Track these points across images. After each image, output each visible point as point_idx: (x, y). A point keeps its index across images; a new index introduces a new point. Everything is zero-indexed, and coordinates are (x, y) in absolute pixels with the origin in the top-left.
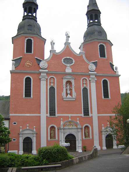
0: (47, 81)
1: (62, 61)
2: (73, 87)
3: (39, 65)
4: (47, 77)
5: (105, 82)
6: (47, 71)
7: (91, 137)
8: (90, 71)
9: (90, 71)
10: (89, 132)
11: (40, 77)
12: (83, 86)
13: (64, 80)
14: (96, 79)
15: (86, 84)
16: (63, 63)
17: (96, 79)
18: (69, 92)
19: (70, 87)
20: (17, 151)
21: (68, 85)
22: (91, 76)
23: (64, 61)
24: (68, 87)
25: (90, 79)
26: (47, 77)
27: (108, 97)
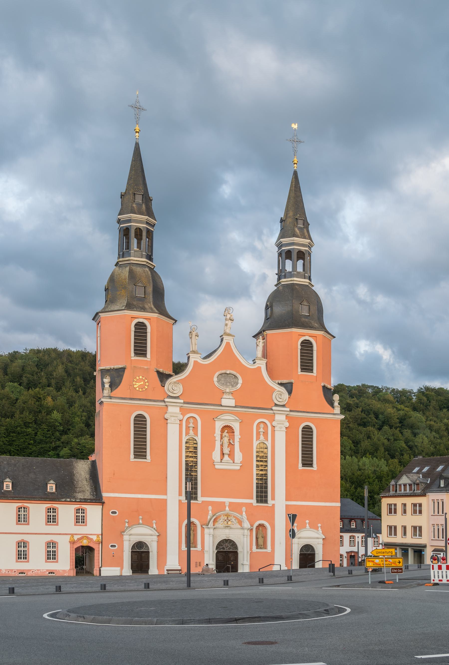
0: (181, 425)
1: (215, 379)
3: (164, 386)
4: (181, 417)
5: (307, 432)
6: (182, 401)
7: (269, 549)
8: (276, 405)
9: (276, 405)
10: (265, 538)
11: (166, 416)
12: (258, 438)
13: (216, 422)
14: (287, 424)
15: (265, 434)
16: (216, 383)
17: (287, 424)
18: (226, 450)
19: (229, 440)
21: (225, 434)
22: (277, 417)
23: (219, 381)
24: (226, 440)
25: (274, 423)
26: (181, 417)
27: (311, 465)
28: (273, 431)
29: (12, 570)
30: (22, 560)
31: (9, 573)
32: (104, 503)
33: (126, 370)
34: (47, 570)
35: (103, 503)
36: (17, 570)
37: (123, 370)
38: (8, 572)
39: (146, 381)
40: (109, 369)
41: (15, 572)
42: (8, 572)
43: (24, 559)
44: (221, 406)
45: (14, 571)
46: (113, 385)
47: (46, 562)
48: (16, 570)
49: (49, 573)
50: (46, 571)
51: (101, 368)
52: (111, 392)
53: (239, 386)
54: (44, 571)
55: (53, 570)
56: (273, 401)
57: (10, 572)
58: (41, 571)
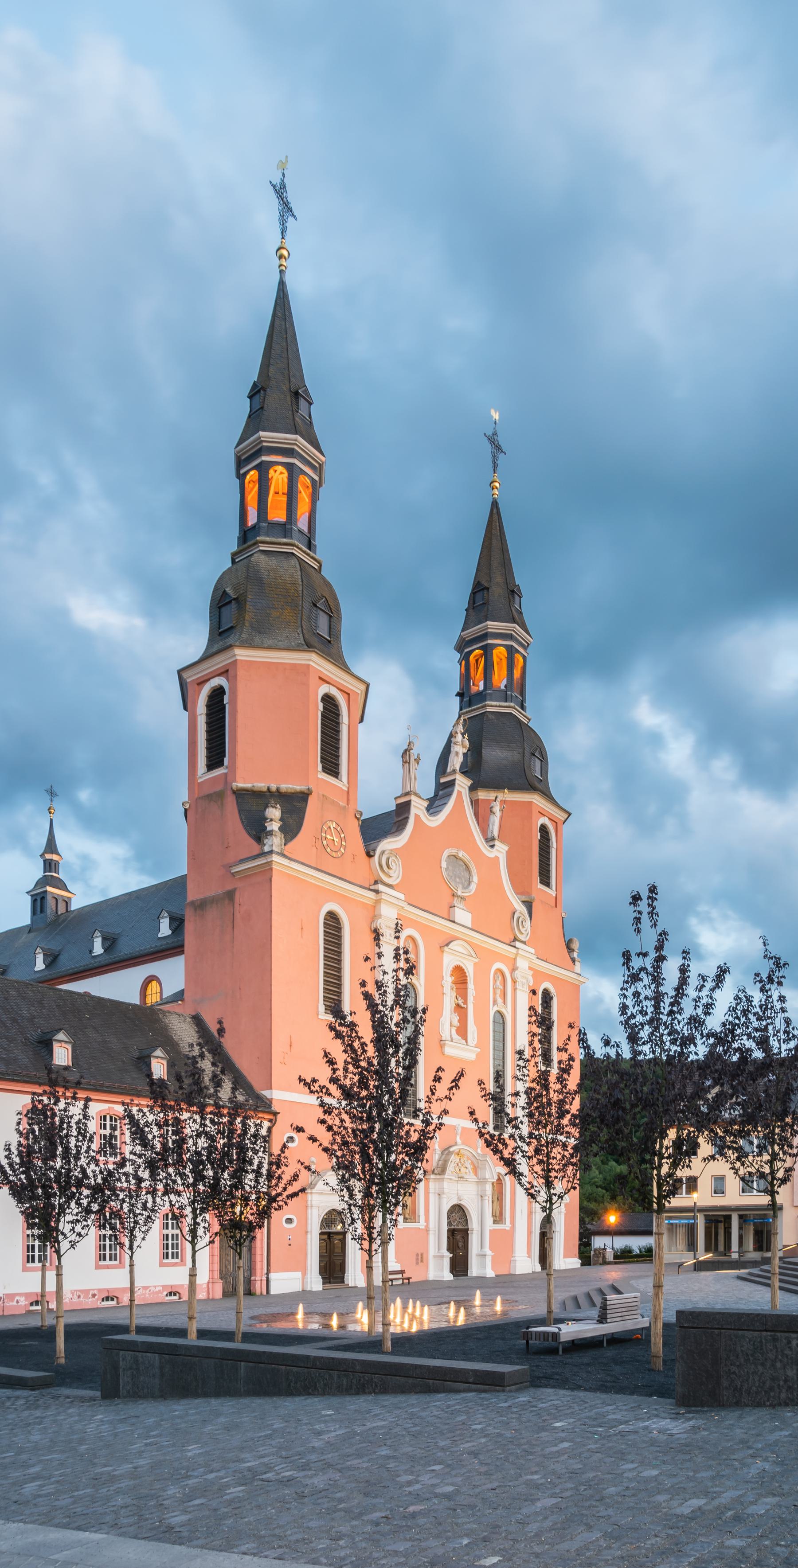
2: (470, 999)
12: (495, 1002)
20: (299, 1274)
28: (515, 989)
29: (86, 1292)
30: (108, 1262)
31: (81, 1299)
32: (275, 1114)
33: (311, 800)
34: (164, 1287)
35: (275, 1114)
36: (100, 1290)
37: (304, 797)
38: (79, 1297)
39: (342, 835)
40: (265, 789)
41: (94, 1296)
42: (79, 1297)
43: (111, 1259)
44: (454, 922)
45: (91, 1292)
46: (291, 830)
47: (162, 1265)
48: (96, 1292)
49: (170, 1294)
50: (161, 1288)
51: (241, 785)
52: (285, 844)
53: (473, 887)
54: (157, 1289)
55: (176, 1286)
56: (513, 929)
57: (82, 1296)
58: (152, 1289)
